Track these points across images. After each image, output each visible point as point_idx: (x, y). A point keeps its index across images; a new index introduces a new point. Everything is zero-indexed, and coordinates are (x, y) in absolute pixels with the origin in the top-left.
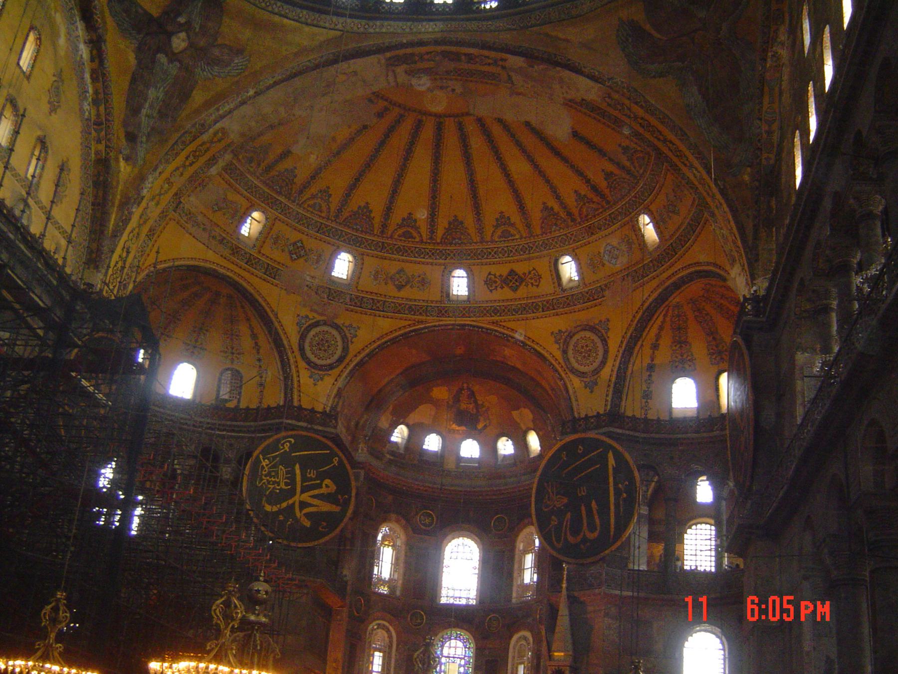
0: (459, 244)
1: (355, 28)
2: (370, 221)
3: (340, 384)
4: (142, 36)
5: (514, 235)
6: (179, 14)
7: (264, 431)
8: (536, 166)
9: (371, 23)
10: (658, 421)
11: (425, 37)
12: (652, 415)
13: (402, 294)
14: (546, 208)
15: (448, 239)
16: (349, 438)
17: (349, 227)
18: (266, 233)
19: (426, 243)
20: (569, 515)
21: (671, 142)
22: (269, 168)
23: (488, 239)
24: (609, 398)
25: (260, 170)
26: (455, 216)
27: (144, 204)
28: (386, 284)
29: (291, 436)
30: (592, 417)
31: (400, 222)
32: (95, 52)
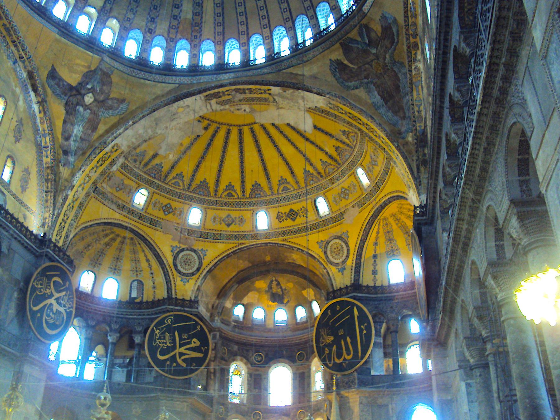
1: (186, 82)
3: (199, 283)
4: (67, 97)
5: (289, 189)
6: (87, 84)
7: (156, 314)
8: (297, 148)
9: (194, 78)
10: (382, 286)
12: (378, 284)
13: (231, 228)
14: (305, 171)
16: (209, 314)
17: (196, 194)
18: (148, 202)
20: (334, 347)
22: (146, 165)
23: (276, 192)
24: (353, 277)
25: (142, 166)
27: (74, 190)
28: (221, 224)
29: (171, 315)
30: (343, 288)
31: (225, 188)
32: (41, 108)
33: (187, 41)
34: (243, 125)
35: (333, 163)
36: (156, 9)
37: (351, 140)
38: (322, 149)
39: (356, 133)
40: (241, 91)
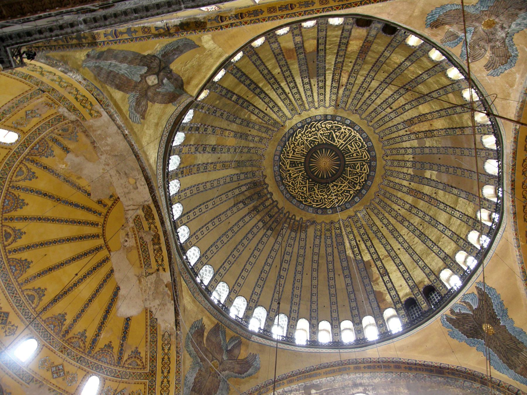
0: (12, 271)
1: (159, 181)
2: (14, 209)
6: (169, 79)
8: (90, 301)
9: (162, 189)
11: (166, 224)
14: (63, 316)
15: (13, 262)
17: (5, 197)
19: (5, 249)
21: (168, 382)
23: (23, 288)
26: (32, 262)
31: (17, 228)
32: (162, 31)
33: (178, 164)
34: (104, 238)
35: (87, 344)
36: (205, 131)
37: (129, 361)
38: (100, 329)
39: (144, 368)
40: (156, 241)
